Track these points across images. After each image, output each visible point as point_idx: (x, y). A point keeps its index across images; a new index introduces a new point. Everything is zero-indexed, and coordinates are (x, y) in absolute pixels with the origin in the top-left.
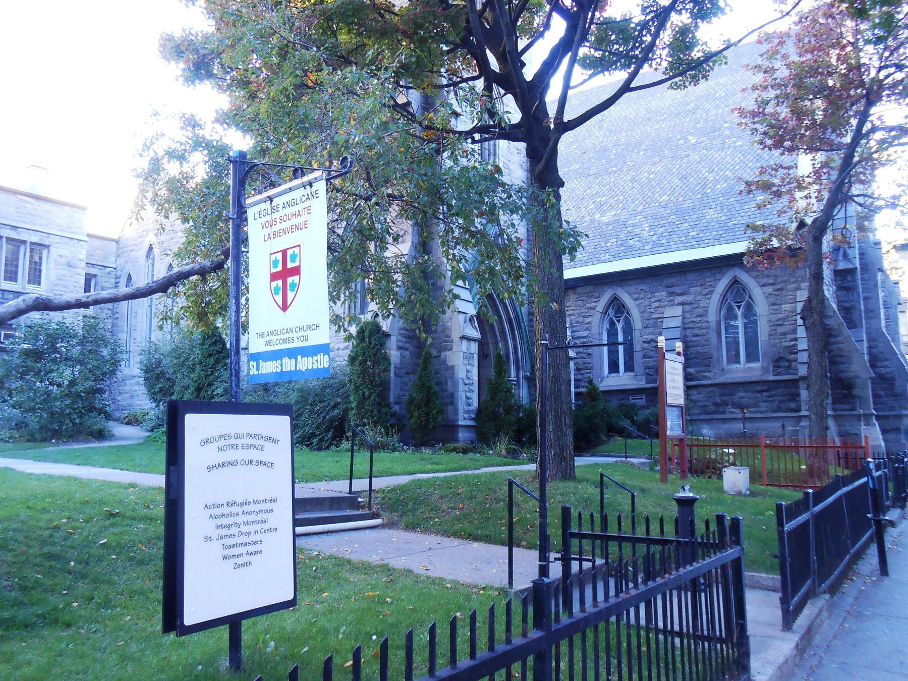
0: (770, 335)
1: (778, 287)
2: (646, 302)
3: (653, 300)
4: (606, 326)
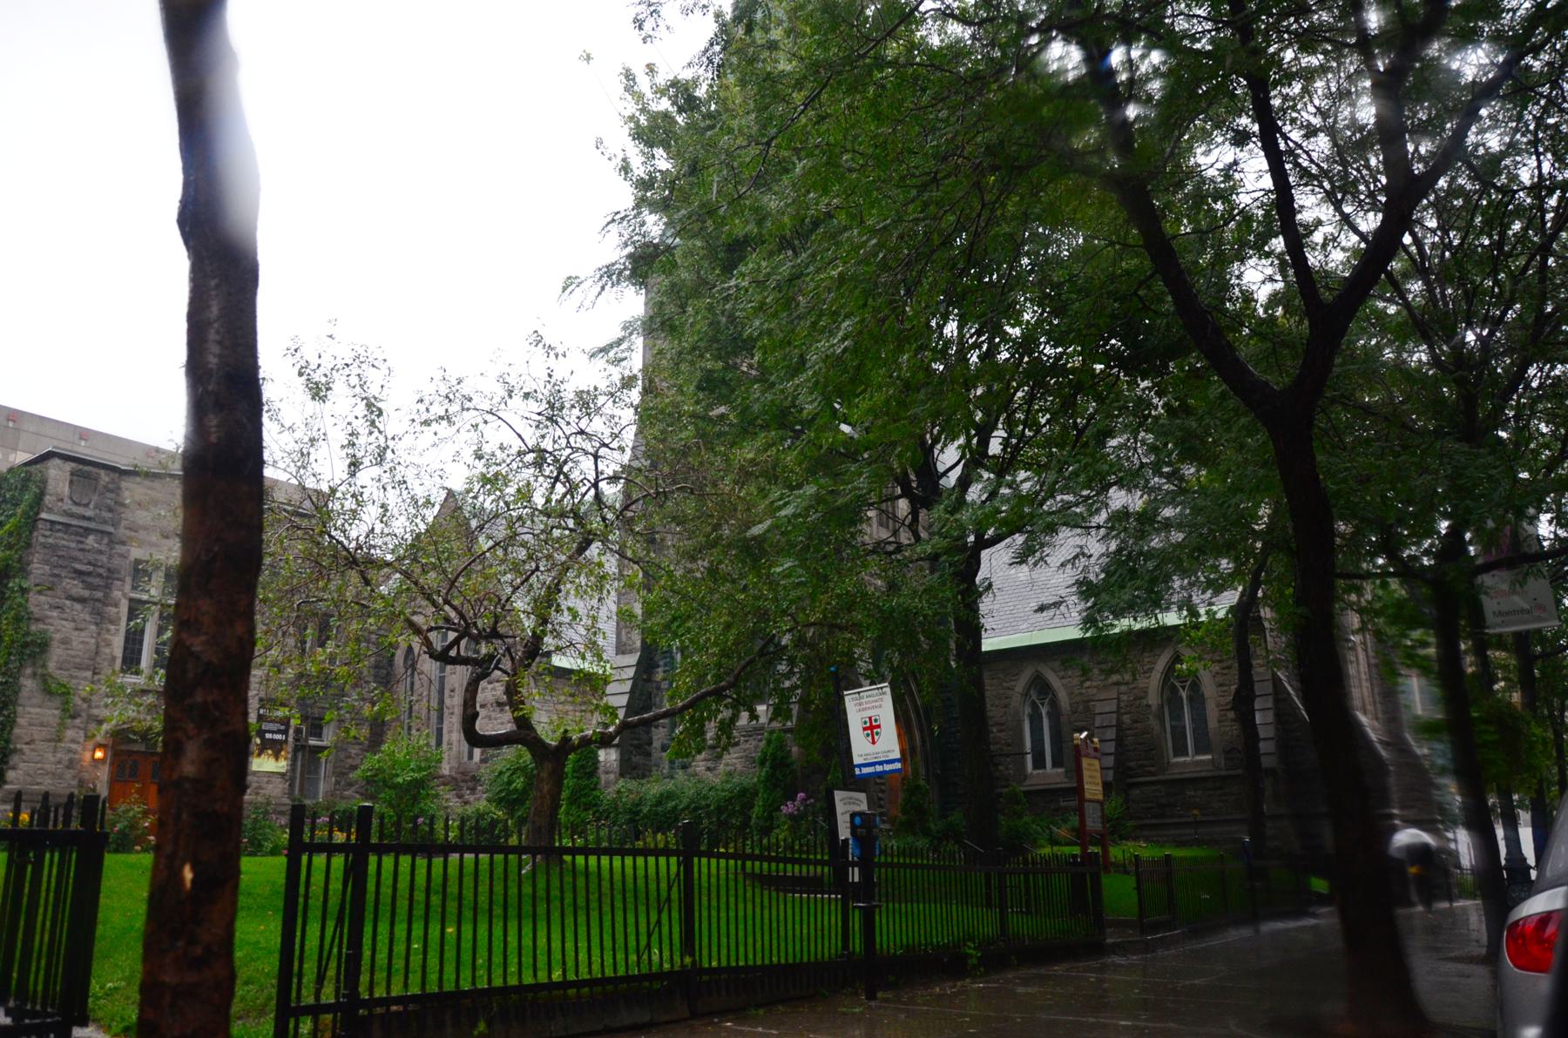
0: (1220, 722)
1: (1225, 665)
4: (1028, 710)
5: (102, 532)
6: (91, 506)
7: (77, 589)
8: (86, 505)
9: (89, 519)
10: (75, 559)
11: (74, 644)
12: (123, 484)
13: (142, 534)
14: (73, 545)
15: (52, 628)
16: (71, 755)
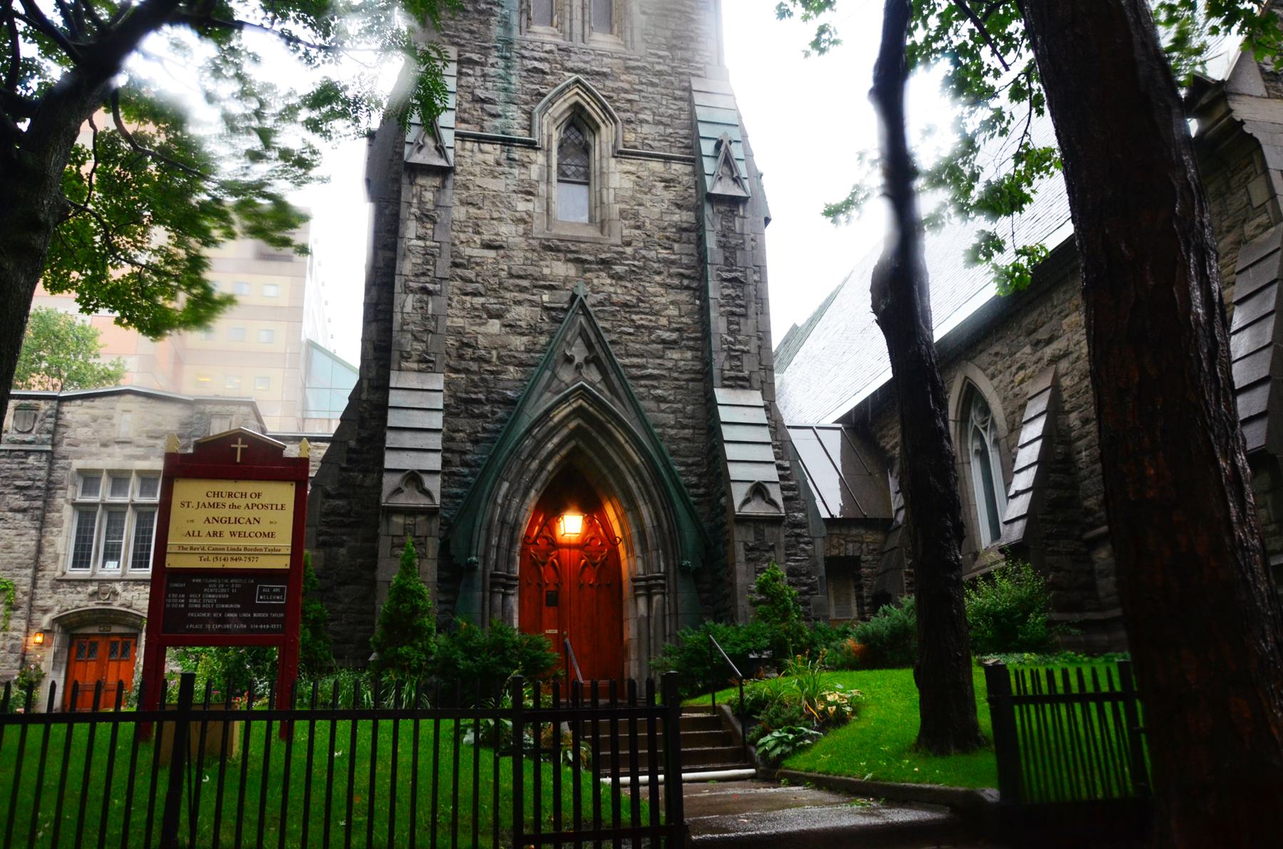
2: (1007, 377)
3: (1014, 369)
5: (41, 452)
6: (34, 432)
7: (18, 501)
8: (29, 432)
11: (16, 547)
12: (65, 409)
13: (83, 447)
14: (15, 466)
16: (13, 642)
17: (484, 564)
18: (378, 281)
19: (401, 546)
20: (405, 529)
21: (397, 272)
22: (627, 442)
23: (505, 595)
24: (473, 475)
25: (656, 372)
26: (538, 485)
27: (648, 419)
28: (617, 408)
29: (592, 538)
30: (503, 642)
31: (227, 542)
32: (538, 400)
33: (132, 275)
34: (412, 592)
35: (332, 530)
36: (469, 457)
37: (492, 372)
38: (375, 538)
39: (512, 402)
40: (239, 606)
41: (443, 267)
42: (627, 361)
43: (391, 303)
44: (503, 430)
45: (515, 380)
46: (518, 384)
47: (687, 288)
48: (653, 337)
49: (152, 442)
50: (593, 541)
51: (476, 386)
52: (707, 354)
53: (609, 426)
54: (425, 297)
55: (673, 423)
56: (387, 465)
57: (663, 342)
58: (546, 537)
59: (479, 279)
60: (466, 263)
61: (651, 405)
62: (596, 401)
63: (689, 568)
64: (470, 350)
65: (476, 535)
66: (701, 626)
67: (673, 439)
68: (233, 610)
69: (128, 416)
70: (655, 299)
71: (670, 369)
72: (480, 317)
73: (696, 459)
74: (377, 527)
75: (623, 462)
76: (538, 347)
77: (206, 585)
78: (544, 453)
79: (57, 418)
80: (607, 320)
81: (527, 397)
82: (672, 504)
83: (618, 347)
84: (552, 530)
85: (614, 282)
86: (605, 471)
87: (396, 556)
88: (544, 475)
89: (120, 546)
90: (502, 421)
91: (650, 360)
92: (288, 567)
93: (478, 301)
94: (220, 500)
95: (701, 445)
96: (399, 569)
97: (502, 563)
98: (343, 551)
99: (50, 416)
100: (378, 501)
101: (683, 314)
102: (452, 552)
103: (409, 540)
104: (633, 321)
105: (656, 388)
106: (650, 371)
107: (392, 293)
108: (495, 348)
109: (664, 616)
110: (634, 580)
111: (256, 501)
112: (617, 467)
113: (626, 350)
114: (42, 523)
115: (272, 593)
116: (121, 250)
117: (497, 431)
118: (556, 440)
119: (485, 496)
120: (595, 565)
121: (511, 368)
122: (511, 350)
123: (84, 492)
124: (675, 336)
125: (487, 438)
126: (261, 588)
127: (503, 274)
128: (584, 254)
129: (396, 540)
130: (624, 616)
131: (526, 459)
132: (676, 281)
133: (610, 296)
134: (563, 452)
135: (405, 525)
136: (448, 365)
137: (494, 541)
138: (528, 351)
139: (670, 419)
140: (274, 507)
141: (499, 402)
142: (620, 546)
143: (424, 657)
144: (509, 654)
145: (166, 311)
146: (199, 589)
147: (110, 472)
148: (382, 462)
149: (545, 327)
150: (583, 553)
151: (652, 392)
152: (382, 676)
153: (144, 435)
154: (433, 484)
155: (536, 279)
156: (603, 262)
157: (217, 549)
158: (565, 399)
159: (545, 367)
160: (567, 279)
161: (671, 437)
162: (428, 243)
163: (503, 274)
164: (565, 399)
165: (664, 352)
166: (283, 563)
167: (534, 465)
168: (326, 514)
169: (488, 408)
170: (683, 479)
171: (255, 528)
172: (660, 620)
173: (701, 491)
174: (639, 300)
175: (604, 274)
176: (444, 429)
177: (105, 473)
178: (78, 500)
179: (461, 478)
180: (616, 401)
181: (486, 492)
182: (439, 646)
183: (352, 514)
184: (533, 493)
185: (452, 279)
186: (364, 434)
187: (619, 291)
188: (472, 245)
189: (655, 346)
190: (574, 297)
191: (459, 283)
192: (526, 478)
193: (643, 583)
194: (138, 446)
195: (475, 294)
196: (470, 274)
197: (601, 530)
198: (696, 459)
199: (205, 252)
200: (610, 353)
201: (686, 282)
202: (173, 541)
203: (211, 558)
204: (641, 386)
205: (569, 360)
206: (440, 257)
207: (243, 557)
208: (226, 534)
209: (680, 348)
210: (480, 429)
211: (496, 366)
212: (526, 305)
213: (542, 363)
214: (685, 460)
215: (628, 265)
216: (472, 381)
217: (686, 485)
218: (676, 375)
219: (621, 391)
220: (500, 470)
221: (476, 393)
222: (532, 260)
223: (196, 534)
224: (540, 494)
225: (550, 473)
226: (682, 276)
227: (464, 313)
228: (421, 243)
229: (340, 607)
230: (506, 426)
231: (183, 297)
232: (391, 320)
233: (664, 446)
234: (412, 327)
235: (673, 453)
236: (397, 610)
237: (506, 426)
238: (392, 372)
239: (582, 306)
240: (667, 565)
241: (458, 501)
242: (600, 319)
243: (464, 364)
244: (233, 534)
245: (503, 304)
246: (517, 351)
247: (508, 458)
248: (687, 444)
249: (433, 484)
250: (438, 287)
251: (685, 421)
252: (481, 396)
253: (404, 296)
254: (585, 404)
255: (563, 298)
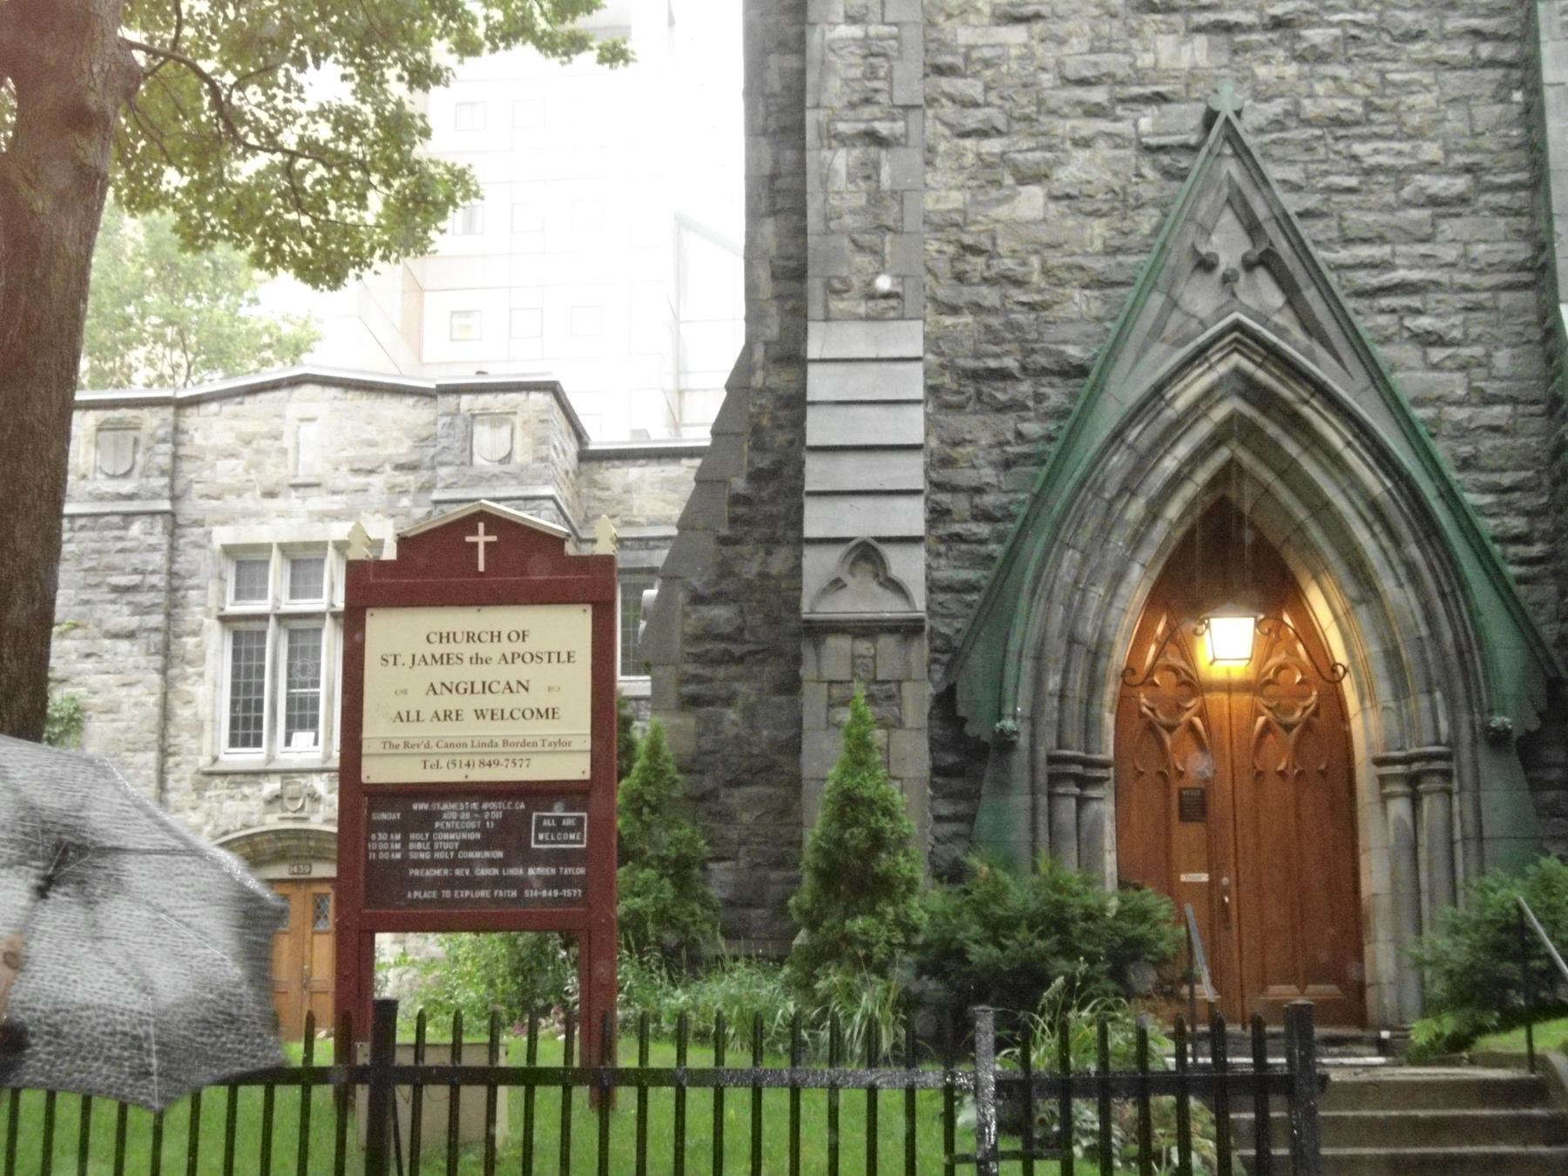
5: (153, 514)
6: (136, 472)
7: (122, 617)
8: (126, 475)
9: (131, 497)
10: (112, 569)
15: (82, 690)
17: (1033, 735)
18: (772, 124)
19: (845, 702)
20: (854, 665)
21: (809, 102)
22: (1349, 444)
23: (1082, 802)
24: (1000, 538)
25: (1415, 275)
26: (1147, 553)
27: (1398, 389)
28: (1324, 369)
29: (1280, 668)
30: (1060, 906)
31: (470, 729)
32: (1138, 360)
33: (272, 169)
34: (870, 803)
35: (707, 672)
36: (988, 500)
37: (1031, 306)
38: (791, 686)
39: (1082, 371)
40: (500, 854)
41: (909, 83)
42: (1344, 255)
43: (800, 169)
44: (1062, 435)
45: (1082, 319)
46: (1091, 328)
47: (1492, 63)
48: (1406, 193)
49: (361, 480)
50: (1283, 674)
51: (997, 340)
52: (1541, 224)
53: (1306, 411)
54: (873, 151)
55: (1460, 392)
56: (810, 531)
57: (1434, 201)
58: (1175, 670)
59: (993, 97)
60: (958, 61)
61: (1408, 353)
62: (1274, 356)
63: (1508, 732)
64: (980, 261)
65: (1010, 671)
66: (1531, 869)
67: (1462, 432)
68: (491, 863)
69: (309, 431)
70: (1411, 100)
71: (1453, 265)
72: (998, 184)
73: (1523, 474)
74: (798, 659)
75: (1344, 491)
76: (1134, 240)
77: (438, 815)
78: (1157, 480)
79: (176, 444)
80: (1292, 162)
81: (1112, 356)
82: (1463, 585)
83: (1320, 224)
84: (1187, 654)
85: (1306, 68)
86: (1301, 514)
87: (838, 726)
88: (1159, 532)
89: (315, 703)
90: (1061, 414)
91: (1401, 249)
92: (587, 776)
93: (993, 146)
94: (451, 648)
95: (1533, 442)
96: (843, 755)
97: (1073, 734)
98: (732, 714)
99: (164, 441)
100: (796, 609)
101: (1479, 130)
102: (962, 711)
103: (859, 691)
104: (1355, 158)
105: (1418, 312)
106: (1400, 275)
107: (802, 149)
108: (1036, 252)
109: (1452, 843)
110: (1380, 762)
111: (519, 647)
112: (1328, 504)
113: (1341, 229)
114: (168, 656)
115: (559, 826)
116: (248, 123)
117: (1050, 438)
118: (1182, 450)
119: (1027, 586)
120: (1288, 728)
121: (1077, 295)
122: (1072, 254)
123: (239, 595)
124: (1460, 184)
125: (1027, 456)
126: (540, 820)
127: (1046, 79)
128: (1231, 9)
129: (837, 692)
130: (1361, 843)
131: (1119, 495)
132: (1461, 51)
133: (1297, 104)
134: (1202, 476)
135: (854, 657)
136: (934, 300)
137: (1053, 682)
138: (1111, 251)
139: (1456, 385)
140: (554, 657)
141: (1052, 373)
142: (1348, 685)
143: (899, 937)
144: (1076, 932)
145: (348, 231)
146: (426, 822)
147: (284, 548)
148: (798, 524)
149: (1148, 192)
150: (1260, 701)
151: (1408, 322)
152: (817, 978)
153: (345, 468)
154: (909, 566)
155: (1122, 83)
156: (1278, 23)
157: (452, 745)
158: (1201, 353)
159: (1151, 285)
160: (1193, 75)
161: (1457, 426)
162: (874, 30)
163: (1046, 79)
164: (1199, 355)
165: (1433, 225)
166: (576, 767)
167: (1136, 509)
168: (696, 639)
169: (1025, 388)
170: (1488, 526)
171: (521, 700)
172: (1440, 852)
173: (1537, 549)
174: (1368, 105)
175: (1280, 54)
176: (934, 443)
177: (275, 551)
178: (233, 608)
179: (974, 547)
180: (1321, 352)
181: (1029, 575)
182: (933, 915)
183: (747, 636)
184: (1136, 572)
185: (931, 102)
186: (765, 462)
187: (1320, 88)
188: (973, 19)
189: (1414, 214)
190: (1210, 117)
191: (949, 110)
192: (1118, 541)
193: (1399, 769)
194: (334, 493)
195: (982, 133)
196: (971, 87)
197: (1300, 648)
198: (1523, 474)
199: (417, 102)
200: (1302, 242)
201: (1485, 50)
202: (374, 729)
203: (443, 763)
204: (1382, 311)
205: (1206, 265)
206: (900, 58)
207: (502, 760)
208: (469, 716)
209: (1475, 212)
210: (1010, 436)
211: (1040, 291)
212: (1101, 144)
213: (1141, 277)
214: (1495, 478)
215: (1340, 24)
216: (988, 329)
217: (1495, 539)
218: (1466, 278)
219: (1331, 328)
220: (1058, 526)
221: (997, 356)
222: (1111, 40)
223: (413, 716)
224: (1155, 574)
225: (1174, 525)
226: (1477, 34)
227: (961, 178)
228: (856, 31)
229: (733, 835)
230: (1066, 424)
231: (375, 201)
232: (802, 212)
233: (1440, 448)
234: (848, 220)
235: (1466, 464)
236: (839, 843)
237: (1066, 424)
238: (811, 325)
239: (1232, 137)
240: (1454, 725)
241: (969, 598)
242: (1277, 161)
243: (966, 294)
244: (480, 714)
245: (1050, 148)
246: (1086, 254)
247: (1072, 499)
248: (1500, 441)
249: (909, 566)
250: (899, 127)
251: (1492, 387)
252: (1010, 363)
253: (826, 153)
254: (1248, 366)
255: (1183, 121)
